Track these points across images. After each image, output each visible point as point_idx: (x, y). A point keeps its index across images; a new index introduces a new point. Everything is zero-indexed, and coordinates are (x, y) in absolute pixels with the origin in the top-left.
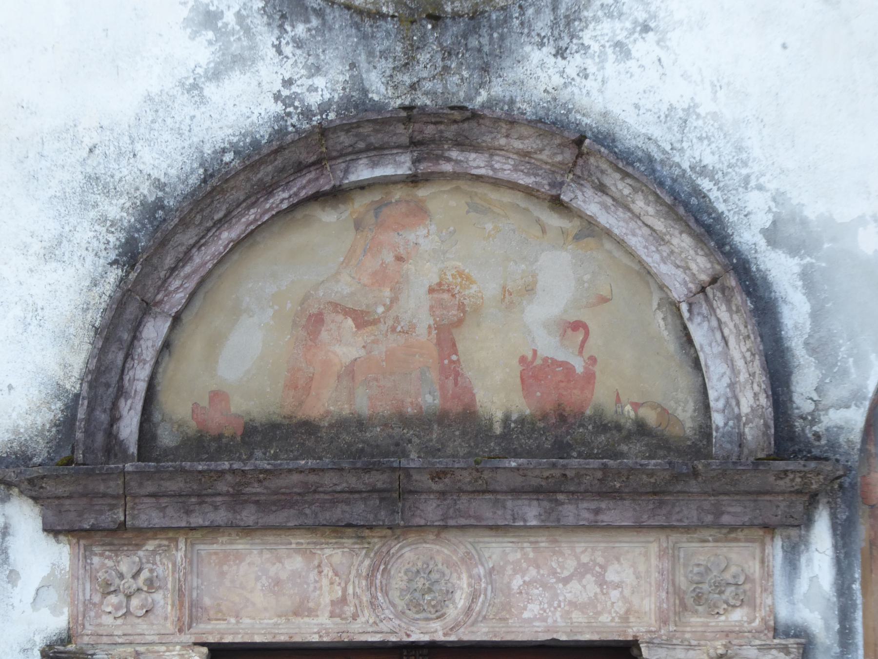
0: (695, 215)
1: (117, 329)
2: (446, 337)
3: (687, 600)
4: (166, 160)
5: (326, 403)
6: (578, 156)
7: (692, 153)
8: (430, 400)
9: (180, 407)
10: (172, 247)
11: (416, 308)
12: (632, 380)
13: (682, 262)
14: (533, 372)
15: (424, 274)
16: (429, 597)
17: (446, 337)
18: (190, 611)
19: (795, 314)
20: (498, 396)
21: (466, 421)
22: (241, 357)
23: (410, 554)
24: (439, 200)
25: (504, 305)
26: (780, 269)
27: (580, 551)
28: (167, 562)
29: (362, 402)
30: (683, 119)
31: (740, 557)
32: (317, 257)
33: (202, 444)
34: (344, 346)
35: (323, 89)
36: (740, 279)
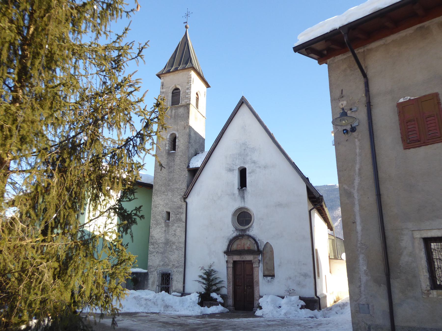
0: (254, 240)
1: (229, 245)
2: (244, 245)
3: (254, 258)
4: (231, 238)
5: (238, 249)
6: (249, 236)
7: (255, 236)
8: (243, 249)
9: (232, 249)
10: (232, 241)
11: (242, 244)
12: (252, 248)
13: (254, 242)
14: (248, 247)
15: (243, 242)
16: (243, 258)
17: (244, 245)
18: (232, 259)
19: (259, 244)
20: (246, 248)
21: (245, 250)
22: (235, 247)
23: (242, 256)
24: (244, 239)
25: (247, 244)
26: (259, 242)
27: (250, 256)
28: (231, 257)
29: (240, 249)
30: (254, 235)
31: (257, 256)
32: (238, 242)
33: (233, 251)
34: (239, 246)
35: (238, 234)
36: (256, 243)
